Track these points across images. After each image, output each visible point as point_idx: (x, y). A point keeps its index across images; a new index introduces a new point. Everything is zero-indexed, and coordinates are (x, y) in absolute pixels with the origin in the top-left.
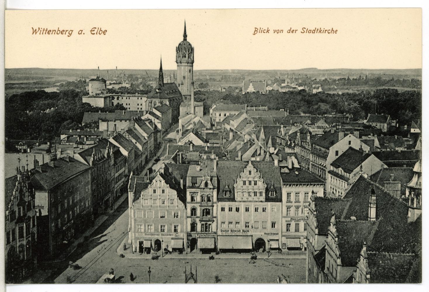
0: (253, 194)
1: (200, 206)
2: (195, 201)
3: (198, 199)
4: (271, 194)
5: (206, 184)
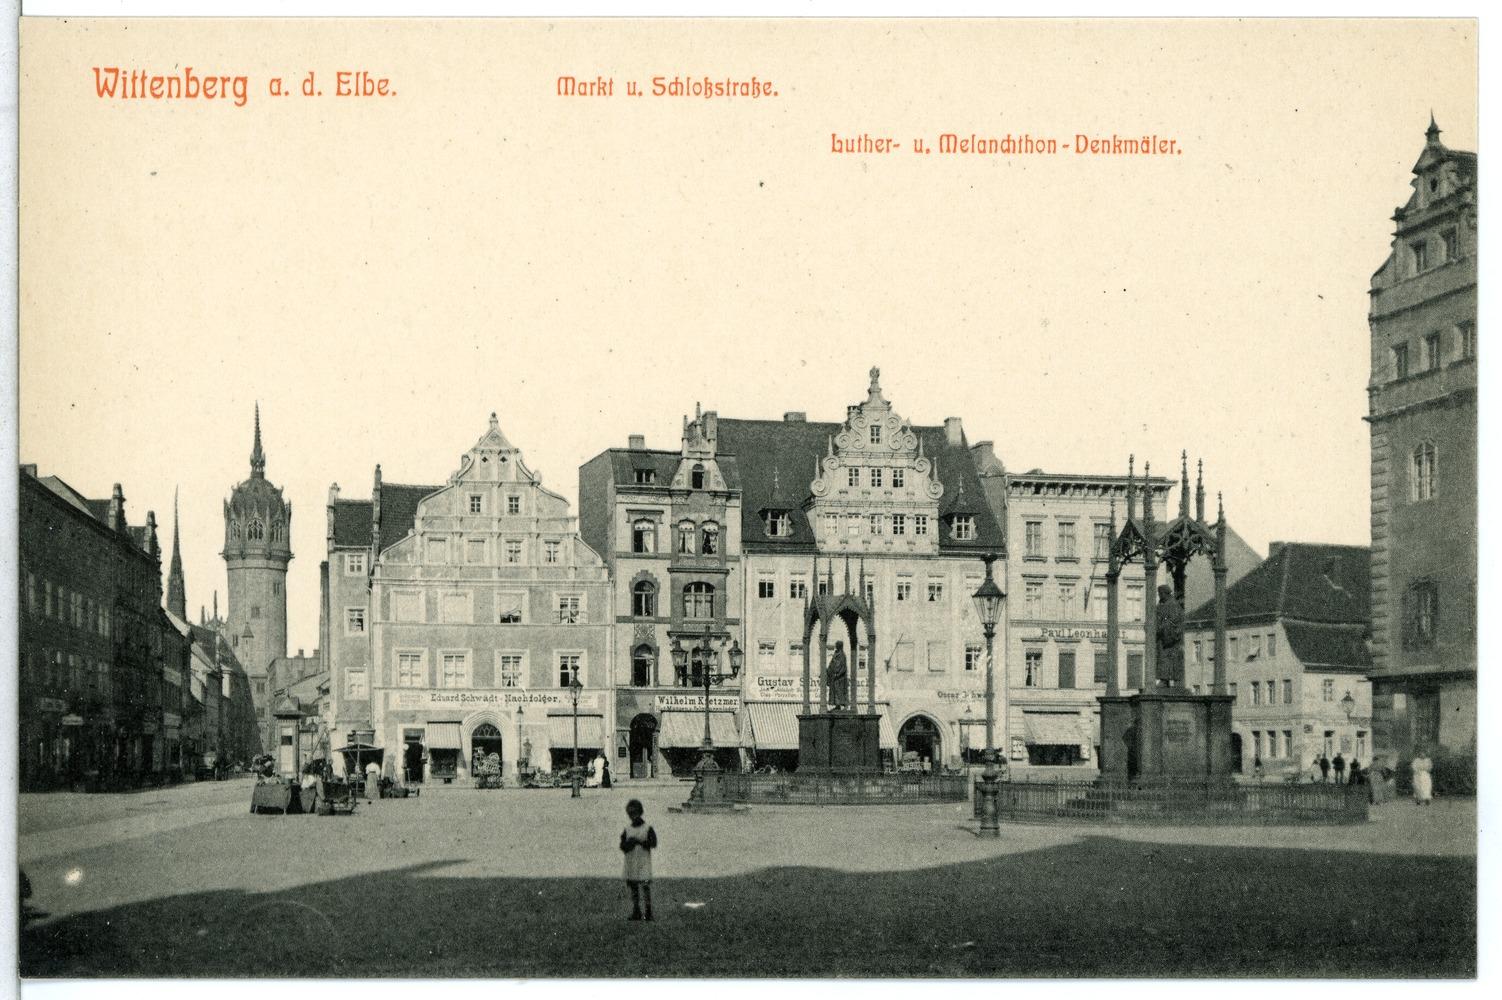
0: (888, 526)
1: (670, 570)
2: (647, 550)
3: (663, 538)
4: (959, 528)
5: (697, 478)
